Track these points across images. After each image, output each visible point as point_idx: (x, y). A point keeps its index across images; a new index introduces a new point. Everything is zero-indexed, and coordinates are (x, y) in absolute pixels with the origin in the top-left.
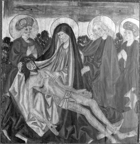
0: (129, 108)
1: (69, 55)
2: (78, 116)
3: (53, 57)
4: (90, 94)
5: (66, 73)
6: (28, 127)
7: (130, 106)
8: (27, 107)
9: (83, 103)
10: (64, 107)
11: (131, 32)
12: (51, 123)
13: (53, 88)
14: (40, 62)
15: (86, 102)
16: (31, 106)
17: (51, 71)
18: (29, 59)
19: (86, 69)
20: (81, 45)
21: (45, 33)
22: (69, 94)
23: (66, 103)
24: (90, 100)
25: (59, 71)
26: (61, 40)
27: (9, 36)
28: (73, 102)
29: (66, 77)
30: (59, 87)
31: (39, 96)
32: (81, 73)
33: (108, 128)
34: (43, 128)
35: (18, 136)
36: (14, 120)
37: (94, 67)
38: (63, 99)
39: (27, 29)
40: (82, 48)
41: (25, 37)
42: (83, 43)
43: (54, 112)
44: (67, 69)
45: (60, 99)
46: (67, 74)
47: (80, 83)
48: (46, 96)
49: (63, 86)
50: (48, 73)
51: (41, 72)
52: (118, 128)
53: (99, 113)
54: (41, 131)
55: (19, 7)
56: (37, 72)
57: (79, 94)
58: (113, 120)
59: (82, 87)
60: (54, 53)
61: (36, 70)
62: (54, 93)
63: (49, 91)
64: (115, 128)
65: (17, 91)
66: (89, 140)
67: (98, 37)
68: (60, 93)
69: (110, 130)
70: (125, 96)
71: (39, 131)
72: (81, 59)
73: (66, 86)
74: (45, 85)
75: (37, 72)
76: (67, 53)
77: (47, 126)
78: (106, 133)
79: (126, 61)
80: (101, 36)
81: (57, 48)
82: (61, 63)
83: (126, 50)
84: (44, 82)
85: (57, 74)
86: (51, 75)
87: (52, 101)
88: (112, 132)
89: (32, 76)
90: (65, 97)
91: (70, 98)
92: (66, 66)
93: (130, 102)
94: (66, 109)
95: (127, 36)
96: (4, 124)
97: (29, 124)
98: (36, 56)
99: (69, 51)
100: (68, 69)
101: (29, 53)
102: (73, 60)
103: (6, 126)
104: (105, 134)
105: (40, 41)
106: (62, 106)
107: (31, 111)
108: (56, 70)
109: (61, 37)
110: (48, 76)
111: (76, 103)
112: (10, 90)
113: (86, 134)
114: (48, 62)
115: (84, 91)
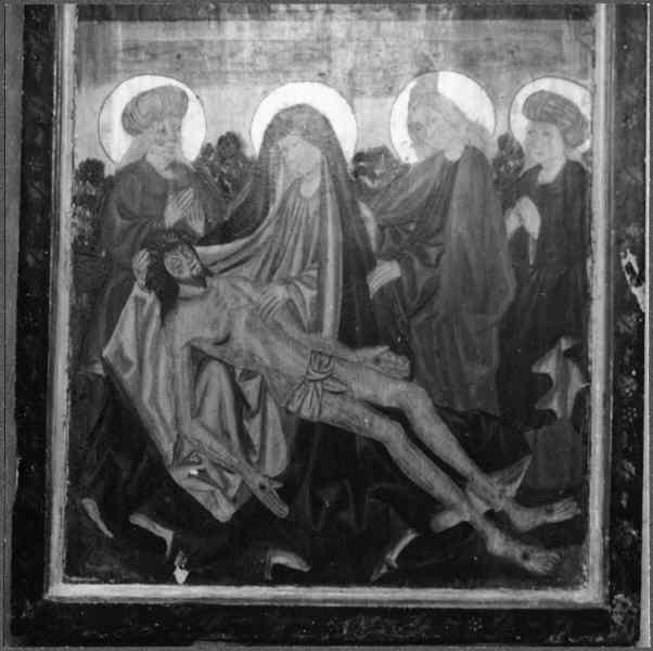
0: (551, 412)
1: (323, 217)
2: (359, 445)
3: (264, 229)
4: (403, 364)
5: (309, 286)
6: (177, 490)
7: (555, 405)
8: (169, 417)
9: (375, 396)
10: (305, 414)
11: (554, 130)
12: (258, 472)
13: (265, 342)
14: (215, 250)
15: (390, 391)
16: (185, 410)
17: (256, 281)
18: (172, 239)
19: (385, 273)
20: (365, 185)
21: (230, 144)
22: (326, 367)
23: (315, 398)
24: (402, 386)
25: (286, 282)
26: (293, 167)
27: (101, 157)
28: (341, 393)
29: (311, 304)
30: (289, 339)
31: (216, 376)
32: (366, 287)
33: (472, 490)
34: (232, 492)
35: (140, 521)
36: (124, 464)
37: (417, 265)
38: (303, 382)
39: (164, 131)
40: (368, 195)
41: (157, 160)
42: (373, 177)
43: (270, 433)
44: (314, 273)
45: (291, 384)
46: (315, 293)
47: (363, 324)
48: (238, 372)
49: (304, 336)
50: (247, 288)
51: (219, 284)
52: (512, 490)
53: (438, 435)
54: (223, 502)
55: (133, 49)
57: (359, 365)
58: (490, 459)
59: (372, 341)
60: (265, 213)
61: (200, 280)
62: (267, 362)
63: (252, 355)
64: (498, 491)
65: (130, 353)
66: (405, 535)
67: (428, 152)
68: (291, 361)
69: (481, 498)
70: (535, 369)
71: (217, 503)
72: (365, 237)
73: (313, 337)
74: (234, 334)
75: (205, 286)
76: (315, 213)
77: (243, 482)
78: (465, 506)
79: (536, 237)
80: (441, 147)
82: (294, 249)
83: (533, 198)
84: (230, 323)
85: (280, 292)
86: (256, 297)
87: (263, 390)
88: (488, 502)
89: (187, 299)
90: (310, 377)
91: (326, 382)
92: (313, 262)
93: (556, 390)
94: (315, 419)
95: (539, 144)
96: (88, 478)
97: (184, 476)
98: (198, 227)
99: (322, 207)
100: (319, 274)
102: (337, 241)
103: (93, 485)
104: (459, 512)
106: (300, 409)
107: (186, 429)
108: (275, 277)
109: (291, 156)
110: (244, 301)
111: (352, 398)
112: (106, 352)
113: (392, 511)
114: (245, 247)
115: (382, 353)
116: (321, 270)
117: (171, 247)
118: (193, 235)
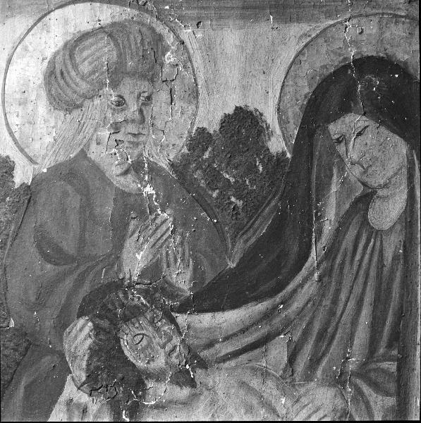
3: (301, 286)
5: (387, 394)
14: (206, 320)
25: (338, 381)
39: (121, 103)
41: (108, 158)
44: (392, 367)
46: (391, 401)
56: (192, 383)
60: (304, 256)
76: (396, 258)
81: (328, 228)
82: (354, 322)
92: (390, 346)
98: (182, 279)
100: (399, 369)
101: (136, 260)
105: (214, 178)
109: (353, 151)
116: (403, 362)
117: (133, 313)
118: (171, 292)
